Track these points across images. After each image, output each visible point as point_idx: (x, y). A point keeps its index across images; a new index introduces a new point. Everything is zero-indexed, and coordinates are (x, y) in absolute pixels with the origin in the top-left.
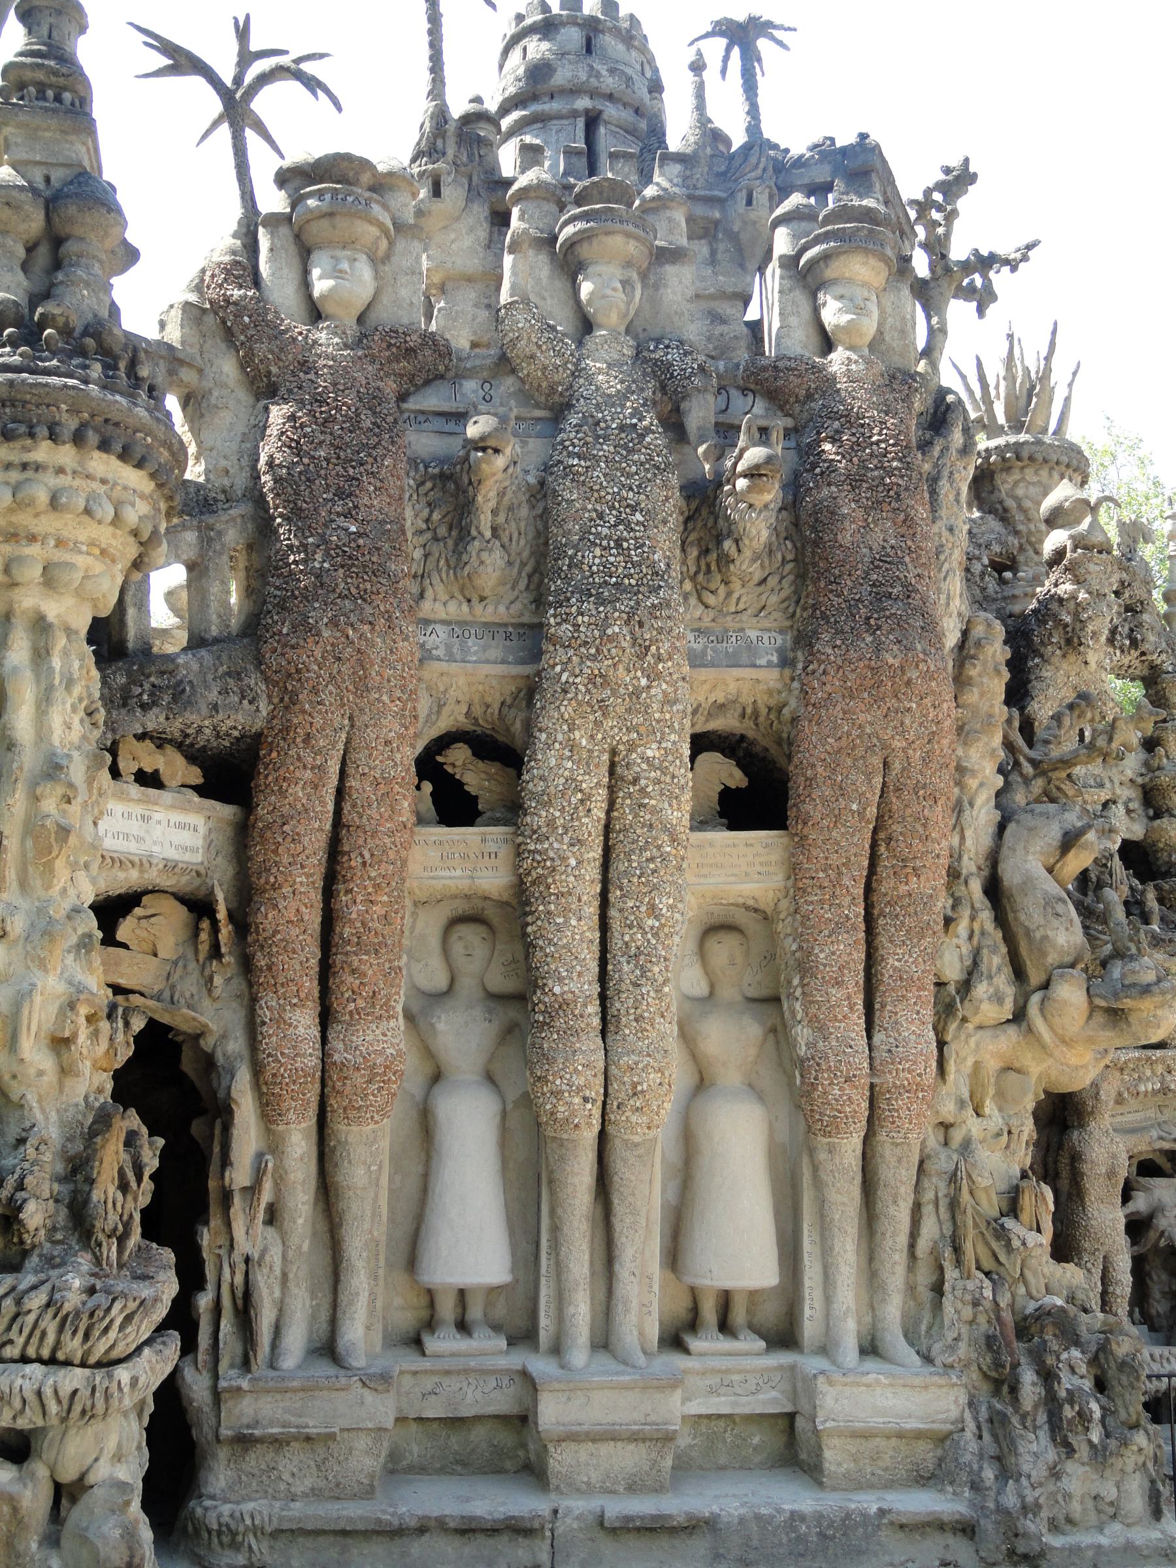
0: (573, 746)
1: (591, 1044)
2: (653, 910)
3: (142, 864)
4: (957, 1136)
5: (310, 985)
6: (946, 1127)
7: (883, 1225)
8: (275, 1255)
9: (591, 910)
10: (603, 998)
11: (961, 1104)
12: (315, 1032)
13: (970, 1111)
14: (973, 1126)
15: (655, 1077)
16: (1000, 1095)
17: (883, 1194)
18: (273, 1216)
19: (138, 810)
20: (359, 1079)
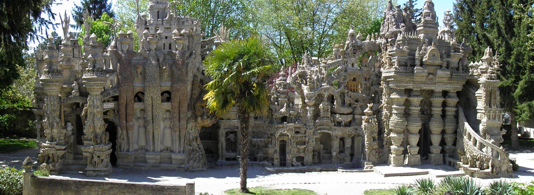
0: (148, 96)
1: (151, 124)
2: (157, 111)
3: (108, 109)
4: (189, 132)
5: (124, 118)
6: (188, 131)
7: (181, 141)
8: (123, 142)
9: (151, 111)
10: (153, 119)
11: (190, 129)
12: (125, 123)
13: (191, 130)
14: (191, 131)
15: (157, 127)
16: (195, 129)
17: (181, 138)
18: (123, 139)
19: (107, 104)
20: (129, 127)
